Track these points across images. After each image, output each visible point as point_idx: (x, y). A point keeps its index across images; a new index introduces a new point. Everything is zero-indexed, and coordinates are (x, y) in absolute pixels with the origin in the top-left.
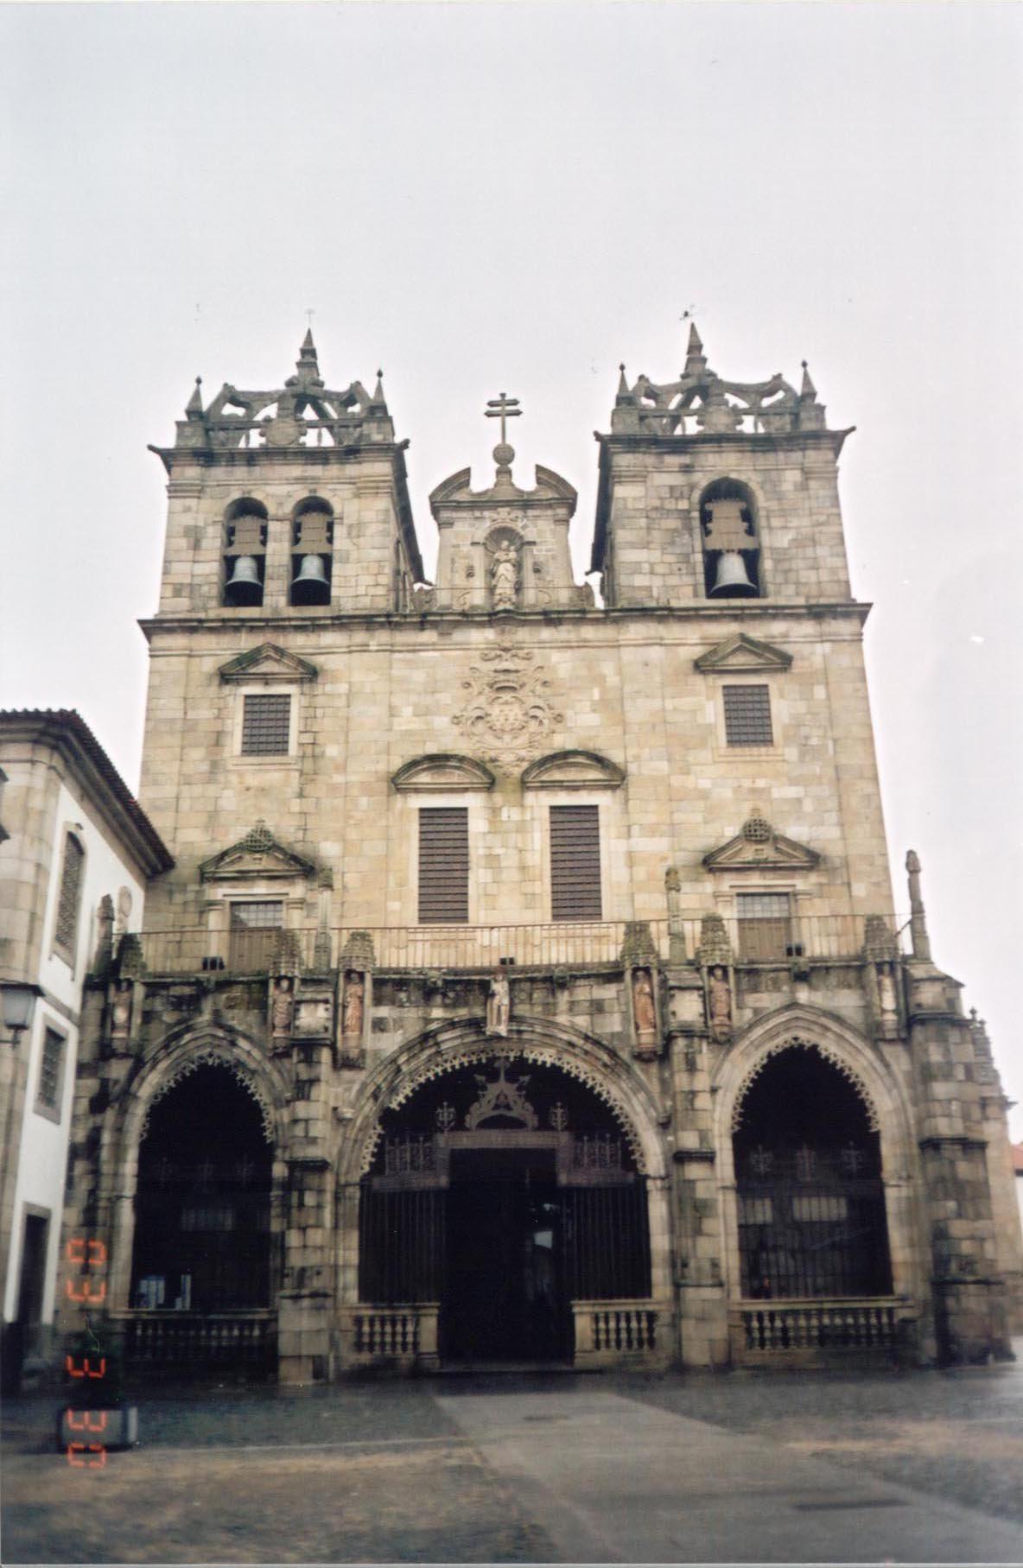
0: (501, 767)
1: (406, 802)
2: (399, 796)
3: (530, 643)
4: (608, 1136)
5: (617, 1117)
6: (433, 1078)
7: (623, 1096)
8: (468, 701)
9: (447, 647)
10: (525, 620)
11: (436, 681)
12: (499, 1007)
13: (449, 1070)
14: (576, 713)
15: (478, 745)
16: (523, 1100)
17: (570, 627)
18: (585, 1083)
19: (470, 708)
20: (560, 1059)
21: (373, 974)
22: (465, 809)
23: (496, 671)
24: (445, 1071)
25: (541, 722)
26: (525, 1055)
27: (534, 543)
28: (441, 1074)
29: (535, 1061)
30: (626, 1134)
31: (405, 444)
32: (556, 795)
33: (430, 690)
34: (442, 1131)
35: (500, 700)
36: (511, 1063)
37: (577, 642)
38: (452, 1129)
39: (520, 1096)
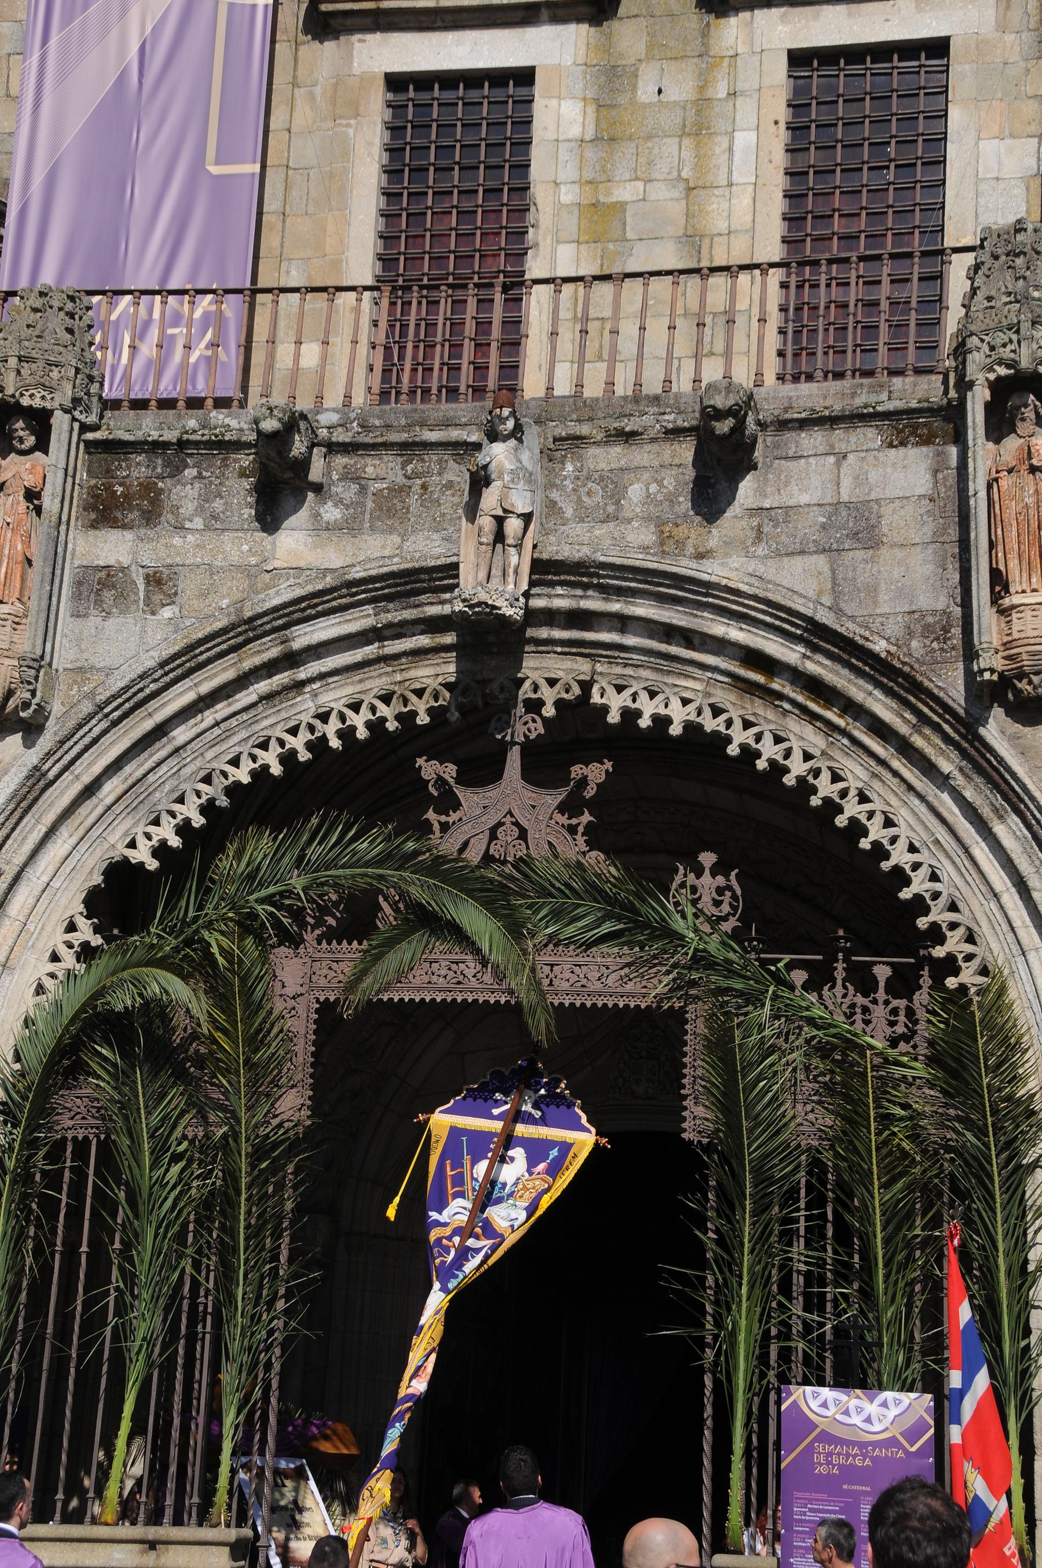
1: (350, 58)
2: (330, 45)
4: (882, 972)
5: (919, 905)
6: (276, 770)
7: (942, 834)
12: (500, 521)
13: (335, 743)
16: (581, 839)
18: (805, 787)
20: (717, 711)
21: (84, 428)
22: (525, 76)
24: (319, 745)
26: (596, 698)
28: (304, 756)
29: (630, 715)
30: (950, 965)
32: (816, 17)
34: (294, 941)
36: (545, 720)
38: (331, 936)
39: (572, 830)
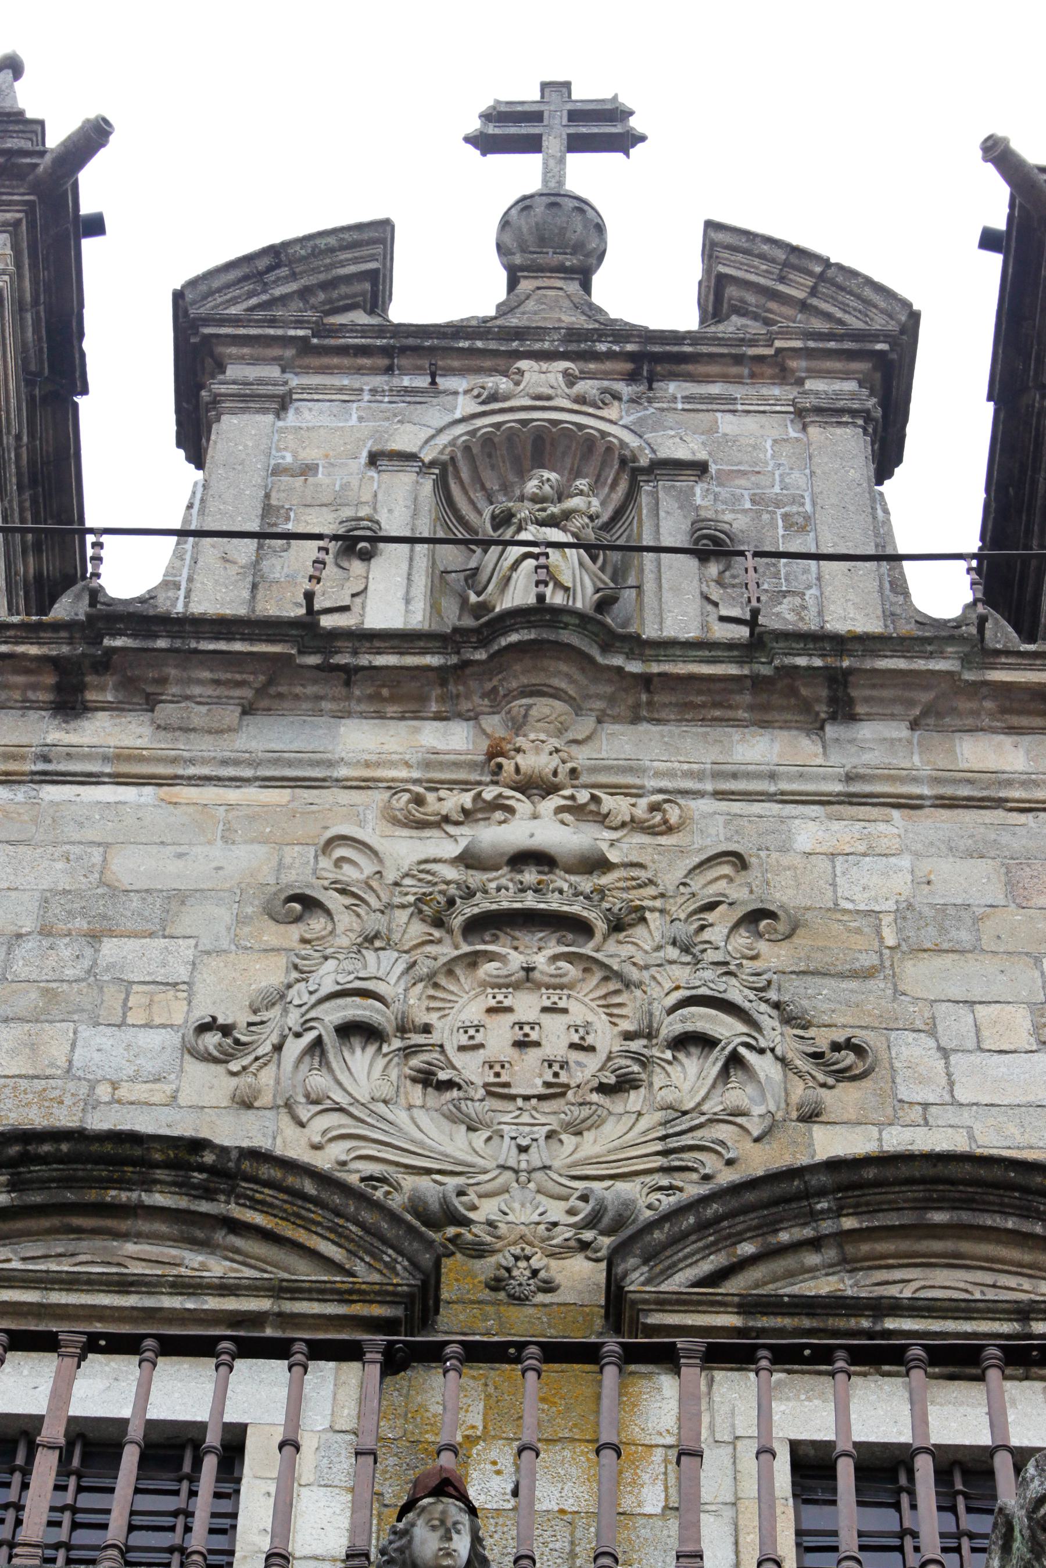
0: (479, 1251)
3: (671, 774)
8: (303, 973)
9: (191, 771)
10: (646, 681)
11: (115, 892)
14: (945, 1053)
15: (337, 1151)
17: (899, 731)
19: (299, 994)
23: (468, 860)
25: (735, 1061)
27: (700, 468)
31: (95, 226)
33: (80, 924)
35: (488, 969)
37: (936, 781)
